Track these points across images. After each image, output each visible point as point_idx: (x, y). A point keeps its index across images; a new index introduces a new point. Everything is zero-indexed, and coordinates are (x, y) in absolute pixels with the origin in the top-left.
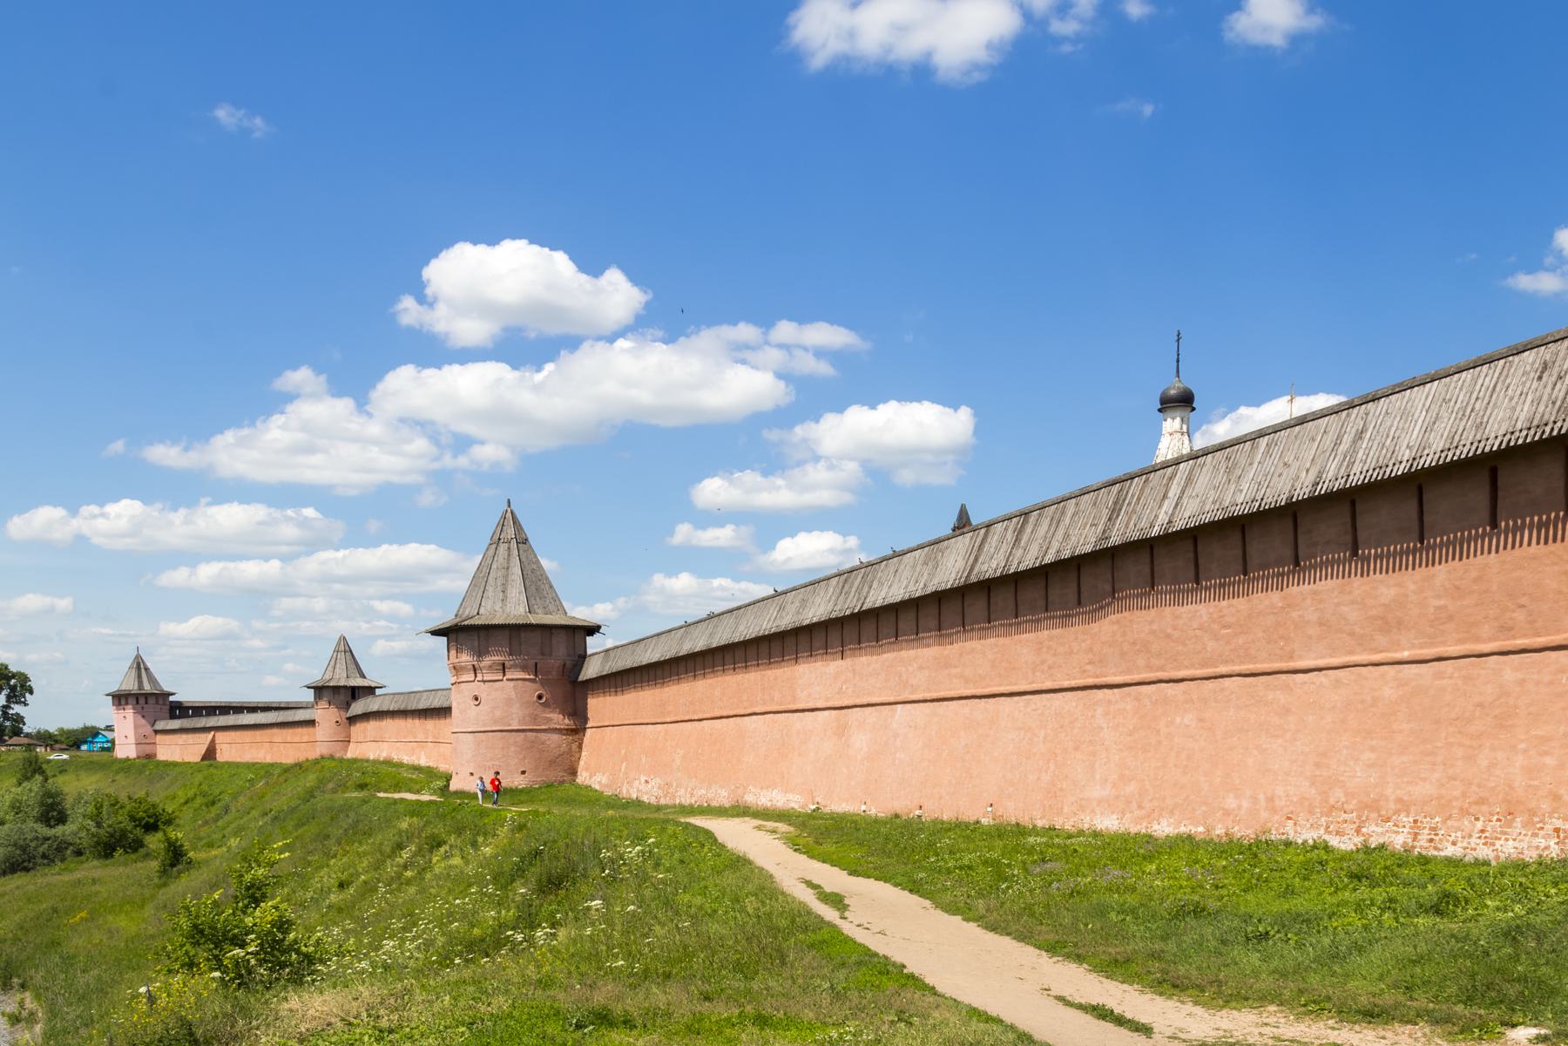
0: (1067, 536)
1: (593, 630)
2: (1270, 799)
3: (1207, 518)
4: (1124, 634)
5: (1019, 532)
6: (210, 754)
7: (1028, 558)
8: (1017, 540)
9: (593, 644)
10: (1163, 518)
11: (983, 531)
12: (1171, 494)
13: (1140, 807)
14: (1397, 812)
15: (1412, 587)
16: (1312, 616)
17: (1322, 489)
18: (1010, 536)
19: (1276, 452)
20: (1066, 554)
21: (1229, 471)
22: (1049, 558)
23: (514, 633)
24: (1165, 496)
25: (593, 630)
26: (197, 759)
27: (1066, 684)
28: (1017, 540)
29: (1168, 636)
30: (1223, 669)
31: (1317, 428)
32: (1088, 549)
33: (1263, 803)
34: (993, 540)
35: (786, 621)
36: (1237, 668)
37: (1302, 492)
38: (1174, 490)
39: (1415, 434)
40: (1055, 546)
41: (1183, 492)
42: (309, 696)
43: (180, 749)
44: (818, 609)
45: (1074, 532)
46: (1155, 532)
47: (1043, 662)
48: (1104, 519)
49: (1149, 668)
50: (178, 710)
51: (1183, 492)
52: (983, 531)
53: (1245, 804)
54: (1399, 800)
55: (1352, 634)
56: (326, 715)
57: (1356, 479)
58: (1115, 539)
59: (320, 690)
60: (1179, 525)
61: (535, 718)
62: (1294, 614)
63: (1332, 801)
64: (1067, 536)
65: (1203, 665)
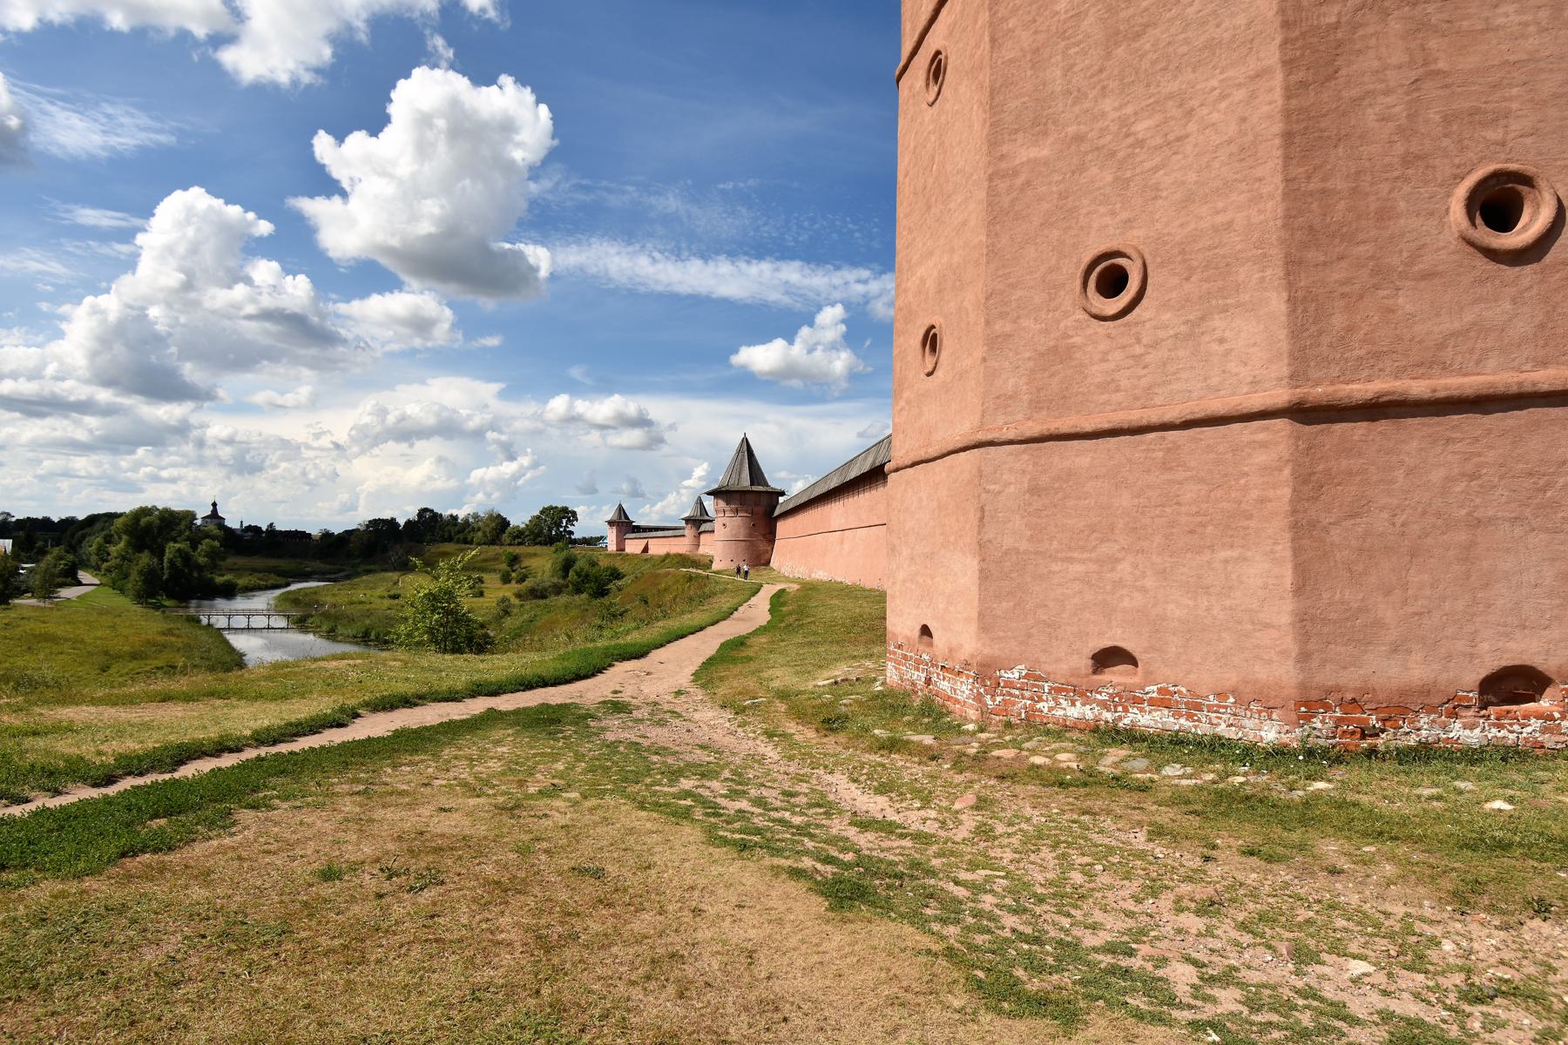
1: (782, 494)
6: (646, 550)
9: (781, 499)
23: (743, 493)
25: (782, 494)
26: (639, 551)
35: (825, 490)
42: (683, 524)
43: (633, 546)
44: (834, 483)
50: (638, 529)
56: (689, 532)
59: (687, 520)
61: (751, 535)
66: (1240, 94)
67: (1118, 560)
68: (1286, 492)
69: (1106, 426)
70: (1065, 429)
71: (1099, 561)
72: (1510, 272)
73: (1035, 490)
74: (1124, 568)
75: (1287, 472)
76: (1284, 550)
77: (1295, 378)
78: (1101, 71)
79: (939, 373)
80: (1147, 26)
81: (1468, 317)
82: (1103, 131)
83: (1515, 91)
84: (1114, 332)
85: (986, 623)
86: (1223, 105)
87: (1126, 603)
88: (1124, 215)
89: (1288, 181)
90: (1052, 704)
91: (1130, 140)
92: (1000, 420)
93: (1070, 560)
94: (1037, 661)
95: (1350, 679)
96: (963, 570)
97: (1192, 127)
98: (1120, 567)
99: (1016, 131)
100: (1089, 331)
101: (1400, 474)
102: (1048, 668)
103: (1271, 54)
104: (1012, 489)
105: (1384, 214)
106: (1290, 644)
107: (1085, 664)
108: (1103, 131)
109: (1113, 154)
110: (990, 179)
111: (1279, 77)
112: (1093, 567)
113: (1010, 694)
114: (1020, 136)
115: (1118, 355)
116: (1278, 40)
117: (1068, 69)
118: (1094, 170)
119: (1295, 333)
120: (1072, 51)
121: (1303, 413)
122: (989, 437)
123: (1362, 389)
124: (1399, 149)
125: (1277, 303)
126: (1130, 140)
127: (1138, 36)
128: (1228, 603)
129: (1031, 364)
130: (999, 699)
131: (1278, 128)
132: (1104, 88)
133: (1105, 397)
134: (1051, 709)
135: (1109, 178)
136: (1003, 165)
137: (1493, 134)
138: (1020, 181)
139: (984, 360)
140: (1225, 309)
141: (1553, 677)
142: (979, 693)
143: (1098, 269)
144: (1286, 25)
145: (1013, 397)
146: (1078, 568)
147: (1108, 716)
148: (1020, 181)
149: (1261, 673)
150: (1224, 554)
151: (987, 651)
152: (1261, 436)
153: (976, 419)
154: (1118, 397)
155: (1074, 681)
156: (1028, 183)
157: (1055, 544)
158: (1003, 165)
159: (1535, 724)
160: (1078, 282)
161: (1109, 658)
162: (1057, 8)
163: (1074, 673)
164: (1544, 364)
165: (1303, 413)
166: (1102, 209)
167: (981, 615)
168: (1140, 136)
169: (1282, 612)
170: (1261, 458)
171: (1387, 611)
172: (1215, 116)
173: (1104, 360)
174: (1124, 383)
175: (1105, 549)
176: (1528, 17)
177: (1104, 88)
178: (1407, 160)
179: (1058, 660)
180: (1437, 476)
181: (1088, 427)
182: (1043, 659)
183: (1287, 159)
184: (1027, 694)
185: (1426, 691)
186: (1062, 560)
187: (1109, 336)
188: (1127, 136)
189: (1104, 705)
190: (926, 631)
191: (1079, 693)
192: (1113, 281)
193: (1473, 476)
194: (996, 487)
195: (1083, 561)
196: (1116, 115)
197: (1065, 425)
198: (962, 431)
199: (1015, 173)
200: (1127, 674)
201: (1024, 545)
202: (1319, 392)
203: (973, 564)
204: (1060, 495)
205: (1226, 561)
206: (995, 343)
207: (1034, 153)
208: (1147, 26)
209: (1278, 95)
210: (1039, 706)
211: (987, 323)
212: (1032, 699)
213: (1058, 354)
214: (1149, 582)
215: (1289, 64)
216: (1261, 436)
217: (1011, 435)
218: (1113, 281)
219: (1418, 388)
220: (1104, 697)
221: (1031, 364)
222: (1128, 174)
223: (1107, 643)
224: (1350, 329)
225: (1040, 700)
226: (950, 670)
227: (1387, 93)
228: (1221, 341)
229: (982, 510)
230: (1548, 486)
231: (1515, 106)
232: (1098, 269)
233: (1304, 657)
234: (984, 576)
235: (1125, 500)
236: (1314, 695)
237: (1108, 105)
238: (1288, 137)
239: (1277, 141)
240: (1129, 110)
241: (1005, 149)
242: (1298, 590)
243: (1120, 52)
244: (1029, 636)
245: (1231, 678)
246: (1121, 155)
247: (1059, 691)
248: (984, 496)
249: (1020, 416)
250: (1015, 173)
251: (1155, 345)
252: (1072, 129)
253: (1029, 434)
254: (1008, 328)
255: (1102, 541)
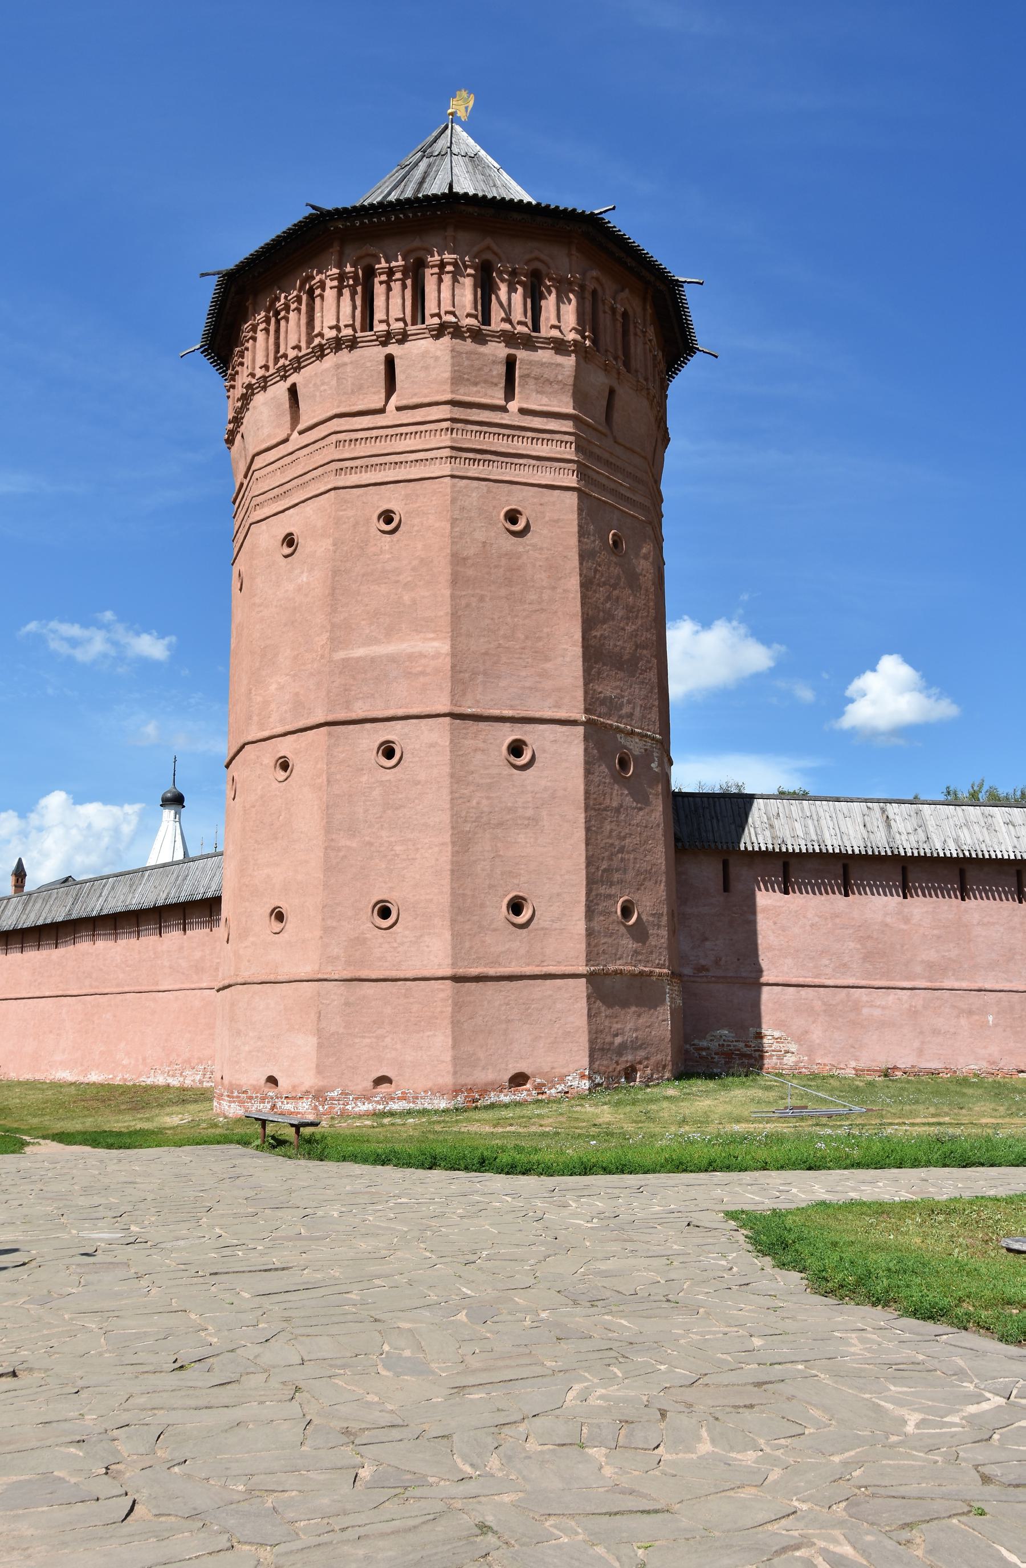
0: (50, 911)
2: (144, 1059)
3: (119, 910)
4: (79, 967)
5: (26, 904)
7: (29, 921)
8: (24, 909)
10: (98, 908)
11: (5, 901)
12: (103, 894)
13: (82, 1065)
14: (198, 1064)
15: (208, 952)
16: (167, 964)
17: (169, 902)
18: (20, 907)
19: (152, 879)
20: (49, 921)
21: (131, 886)
22: (40, 922)
24: (100, 895)
27: (47, 994)
28: (24, 909)
29: (101, 970)
30: (126, 989)
31: (170, 871)
32: (60, 919)
33: (141, 1061)
34: (11, 907)
36: (132, 989)
37: (160, 903)
38: (105, 892)
39: (205, 882)
40: (44, 915)
41: (109, 894)
45: (54, 908)
46: (94, 914)
47: (35, 981)
48: (70, 903)
49: (91, 986)
51: (109, 894)
52: (5, 901)
53: (133, 1062)
54: (199, 1058)
55: (183, 973)
57: (182, 899)
58: (74, 916)
60: (105, 912)
62: (159, 962)
63: (171, 1059)
64: (50, 911)
65: (118, 985)
66: (436, 849)
67: (385, 1037)
68: (450, 1009)
69: (382, 977)
70: (363, 977)
71: (377, 1037)
72: (520, 931)
73: (347, 1004)
74: (388, 1040)
75: (450, 1001)
76: (449, 1032)
77: (454, 965)
78: (381, 817)
79: (284, 935)
80: (401, 806)
81: (507, 946)
82: (381, 845)
83: (523, 866)
84: (385, 935)
85: (320, 1070)
86: (430, 851)
87: (389, 1056)
88: (390, 885)
89: (452, 889)
90: (354, 1105)
91: (393, 852)
92: (330, 969)
93: (363, 1037)
94: (347, 1085)
95: (469, 1081)
96: (306, 1044)
97: (418, 856)
98: (386, 1040)
99: (340, 830)
100: (374, 933)
101: (486, 1003)
102: (352, 1088)
103: (447, 838)
104: (336, 1003)
105: (482, 906)
106: (450, 1068)
107: (369, 1084)
108: (381, 845)
109: (385, 856)
110: (326, 848)
111: (450, 848)
112: (374, 1040)
113: (333, 1104)
114: (342, 833)
115: (386, 946)
116: (450, 833)
117: (366, 811)
118: (377, 861)
119: (454, 947)
120: (368, 803)
121: (456, 979)
122: (325, 977)
123: (474, 971)
124: (487, 882)
125: (447, 935)
126: (393, 852)
127: (397, 809)
128: (429, 1053)
129: (346, 943)
130: (326, 1107)
131: (449, 867)
132: (382, 825)
133: (381, 963)
134: (353, 1108)
135: (384, 866)
136: (333, 844)
137: (516, 881)
138: (341, 854)
139: (321, 937)
140: (429, 934)
141: (529, 1075)
142: (315, 1106)
143: (379, 906)
144: (453, 828)
145: (337, 958)
146: (368, 1041)
147: (381, 1107)
148: (341, 854)
149: (440, 1081)
150: (429, 1033)
151: (321, 1083)
152: (442, 987)
153: (316, 968)
154: (386, 964)
155: (364, 1093)
156: (345, 857)
157: (357, 1030)
158: (333, 844)
159: (525, 1093)
160: (370, 910)
161: (381, 1080)
162: (361, 780)
163: (365, 1090)
164: (528, 965)
165: (456, 979)
166: (381, 879)
167: (318, 1066)
168: (397, 852)
169: (448, 1056)
170: (442, 995)
171: (481, 1054)
172: (427, 855)
173: (380, 947)
174: (389, 958)
175: (380, 1032)
176: (527, 840)
177: (382, 825)
178: (491, 886)
179: (357, 1084)
180: (497, 1003)
181: (374, 977)
182: (350, 1084)
183: (452, 880)
184: (341, 1102)
185: (492, 1083)
186: (360, 1037)
187: (383, 936)
188: (392, 850)
189: (378, 1102)
190: (272, 1080)
191: (367, 1098)
192: (385, 913)
193: (508, 1004)
194: (328, 1002)
195: (370, 1037)
196: (387, 839)
197: (364, 974)
198: (306, 970)
199: (339, 850)
200: (387, 1087)
201: (341, 1030)
202: (461, 971)
203: (313, 1040)
204: (359, 1007)
205: (428, 1036)
206: (327, 930)
207: (348, 843)
208: (401, 806)
209: (449, 854)
210: (347, 1107)
211: (323, 919)
212: (344, 1104)
213: (359, 941)
214: (399, 1046)
215: (453, 843)
216: (442, 987)
217: (336, 977)
218: (385, 913)
219: (492, 972)
220: (378, 1099)
221: (346, 943)
222: (392, 867)
223: (380, 1074)
224: (471, 948)
225: (348, 1104)
226: (294, 1098)
227: (484, 860)
228: (428, 946)
229: (320, 1013)
230: (529, 1008)
231: (522, 872)
232: (379, 906)
233: (455, 1073)
234: (320, 1046)
235: (388, 1010)
236: (458, 1088)
237: (384, 833)
238: (452, 871)
239: (449, 872)
240: (392, 839)
241: (334, 836)
242: (454, 1047)
243: (389, 812)
244: (343, 1074)
245: (430, 1084)
246: (389, 857)
247: (357, 1099)
248: (321, 1006)
249: (340, 968)
250: (339, 850)
251: (402, 944)
252: (367, 839)
253: (345, 977)
254: (334, 924)
255: (378, 1028)
